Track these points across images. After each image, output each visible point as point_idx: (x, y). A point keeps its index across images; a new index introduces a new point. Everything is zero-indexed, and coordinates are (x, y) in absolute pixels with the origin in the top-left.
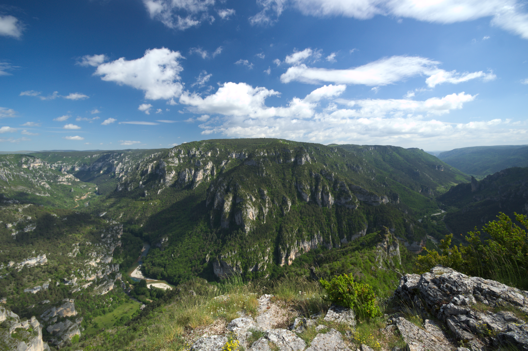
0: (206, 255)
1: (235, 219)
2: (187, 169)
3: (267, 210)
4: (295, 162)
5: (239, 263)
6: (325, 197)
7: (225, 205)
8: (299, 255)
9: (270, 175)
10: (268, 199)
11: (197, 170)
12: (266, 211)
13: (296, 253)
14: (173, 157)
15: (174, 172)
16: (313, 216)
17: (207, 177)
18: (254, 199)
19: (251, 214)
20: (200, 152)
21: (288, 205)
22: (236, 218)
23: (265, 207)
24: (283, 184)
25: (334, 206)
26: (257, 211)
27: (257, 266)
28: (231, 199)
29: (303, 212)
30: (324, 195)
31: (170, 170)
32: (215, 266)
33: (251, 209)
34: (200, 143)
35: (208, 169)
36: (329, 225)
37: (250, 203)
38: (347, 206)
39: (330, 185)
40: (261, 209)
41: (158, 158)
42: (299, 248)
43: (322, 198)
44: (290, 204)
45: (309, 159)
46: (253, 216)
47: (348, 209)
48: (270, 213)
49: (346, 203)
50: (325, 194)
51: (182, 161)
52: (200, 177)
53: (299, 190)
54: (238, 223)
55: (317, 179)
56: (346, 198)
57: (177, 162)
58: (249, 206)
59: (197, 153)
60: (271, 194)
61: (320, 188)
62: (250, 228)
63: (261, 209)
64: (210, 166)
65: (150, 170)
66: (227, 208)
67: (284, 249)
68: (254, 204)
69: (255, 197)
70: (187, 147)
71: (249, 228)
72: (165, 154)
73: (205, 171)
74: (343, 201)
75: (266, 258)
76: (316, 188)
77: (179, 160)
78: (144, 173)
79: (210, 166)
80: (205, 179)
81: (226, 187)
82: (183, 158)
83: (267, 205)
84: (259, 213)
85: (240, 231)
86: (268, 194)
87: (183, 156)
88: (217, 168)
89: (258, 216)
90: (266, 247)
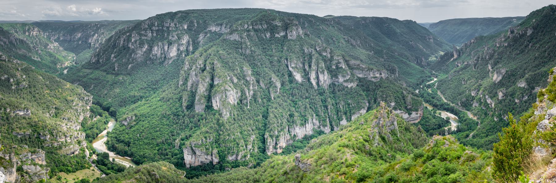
0: (175, 140)
1: (212, 102)
2: (160, 44)
3: (252, 92)
4: (285, 36)
5: (215, 151)
6: (321, 76)
7: (200, 86)
8: (291, 142)
9: (255, 52)
10: (251, 79)
11: (170, 44)
12: (249, 94)
13: (287, 141)
14: (145, 30)
15: (146, 47)
16: (306, 98)
17: (181, 52)
18: (235, 80)
19: (232, 98)
20: (176, 25)
21: (276, 87)
22: (213, 101)
23: (249, 89)
24: (271, 62)
25: (331, 86)
26: (240, 94)
27: (237, 155)
28: (208, 80)
29: (295, 95)
30: (319, 73)
31: (142, 44)
32: (186, 152)
33: (232, 92)
34: (176, 13)
35: (182, 44)
36: (326, 107)
37: (231, 85)
38: (345, 84)
39: (325, 61)
40: (243, 92)
41: (130, 31)
42: (290, 135)
43: (318, 78)
44: (279, 85)
45: (301, 32)
46: (235, 100)
47: (347, 87)
48: (254, 96)
49: (346, 81)
50: (321, 72)
51: (155, 35)
52: (173, 53)
53: (290, 69)
54: (215, 108)
55: (311, 56)
56: (344, 76)
57: (150, 34)
58: (229, 89)
59: (172, 25)
60: (256, 74)
61: (314, 67)
62: (230, 113)
63: (243, 92)
64: (184, 41)
65: (122, 42)
66: (202, 89)
67: (271, 136)
68: (235, 85)
69: (238, 78)
70: (160, 18)
71: (228, 114)
72: (137, 26)
73: (179, 45)
74: (341, 80)
75: (250, 147)
76: (310, 66)
77: (152, 33)
78: (114, 46)
79: (185, 39)
80: (179, 55)
81: (202, 66)
82: (157, 31)
83: (251, 88)
84: (242, 96)
85: (217, 116)
86: (253, 75)
87: (157, 28)
88: (194, 42)
89: (241, 101)
90: (250, 135)
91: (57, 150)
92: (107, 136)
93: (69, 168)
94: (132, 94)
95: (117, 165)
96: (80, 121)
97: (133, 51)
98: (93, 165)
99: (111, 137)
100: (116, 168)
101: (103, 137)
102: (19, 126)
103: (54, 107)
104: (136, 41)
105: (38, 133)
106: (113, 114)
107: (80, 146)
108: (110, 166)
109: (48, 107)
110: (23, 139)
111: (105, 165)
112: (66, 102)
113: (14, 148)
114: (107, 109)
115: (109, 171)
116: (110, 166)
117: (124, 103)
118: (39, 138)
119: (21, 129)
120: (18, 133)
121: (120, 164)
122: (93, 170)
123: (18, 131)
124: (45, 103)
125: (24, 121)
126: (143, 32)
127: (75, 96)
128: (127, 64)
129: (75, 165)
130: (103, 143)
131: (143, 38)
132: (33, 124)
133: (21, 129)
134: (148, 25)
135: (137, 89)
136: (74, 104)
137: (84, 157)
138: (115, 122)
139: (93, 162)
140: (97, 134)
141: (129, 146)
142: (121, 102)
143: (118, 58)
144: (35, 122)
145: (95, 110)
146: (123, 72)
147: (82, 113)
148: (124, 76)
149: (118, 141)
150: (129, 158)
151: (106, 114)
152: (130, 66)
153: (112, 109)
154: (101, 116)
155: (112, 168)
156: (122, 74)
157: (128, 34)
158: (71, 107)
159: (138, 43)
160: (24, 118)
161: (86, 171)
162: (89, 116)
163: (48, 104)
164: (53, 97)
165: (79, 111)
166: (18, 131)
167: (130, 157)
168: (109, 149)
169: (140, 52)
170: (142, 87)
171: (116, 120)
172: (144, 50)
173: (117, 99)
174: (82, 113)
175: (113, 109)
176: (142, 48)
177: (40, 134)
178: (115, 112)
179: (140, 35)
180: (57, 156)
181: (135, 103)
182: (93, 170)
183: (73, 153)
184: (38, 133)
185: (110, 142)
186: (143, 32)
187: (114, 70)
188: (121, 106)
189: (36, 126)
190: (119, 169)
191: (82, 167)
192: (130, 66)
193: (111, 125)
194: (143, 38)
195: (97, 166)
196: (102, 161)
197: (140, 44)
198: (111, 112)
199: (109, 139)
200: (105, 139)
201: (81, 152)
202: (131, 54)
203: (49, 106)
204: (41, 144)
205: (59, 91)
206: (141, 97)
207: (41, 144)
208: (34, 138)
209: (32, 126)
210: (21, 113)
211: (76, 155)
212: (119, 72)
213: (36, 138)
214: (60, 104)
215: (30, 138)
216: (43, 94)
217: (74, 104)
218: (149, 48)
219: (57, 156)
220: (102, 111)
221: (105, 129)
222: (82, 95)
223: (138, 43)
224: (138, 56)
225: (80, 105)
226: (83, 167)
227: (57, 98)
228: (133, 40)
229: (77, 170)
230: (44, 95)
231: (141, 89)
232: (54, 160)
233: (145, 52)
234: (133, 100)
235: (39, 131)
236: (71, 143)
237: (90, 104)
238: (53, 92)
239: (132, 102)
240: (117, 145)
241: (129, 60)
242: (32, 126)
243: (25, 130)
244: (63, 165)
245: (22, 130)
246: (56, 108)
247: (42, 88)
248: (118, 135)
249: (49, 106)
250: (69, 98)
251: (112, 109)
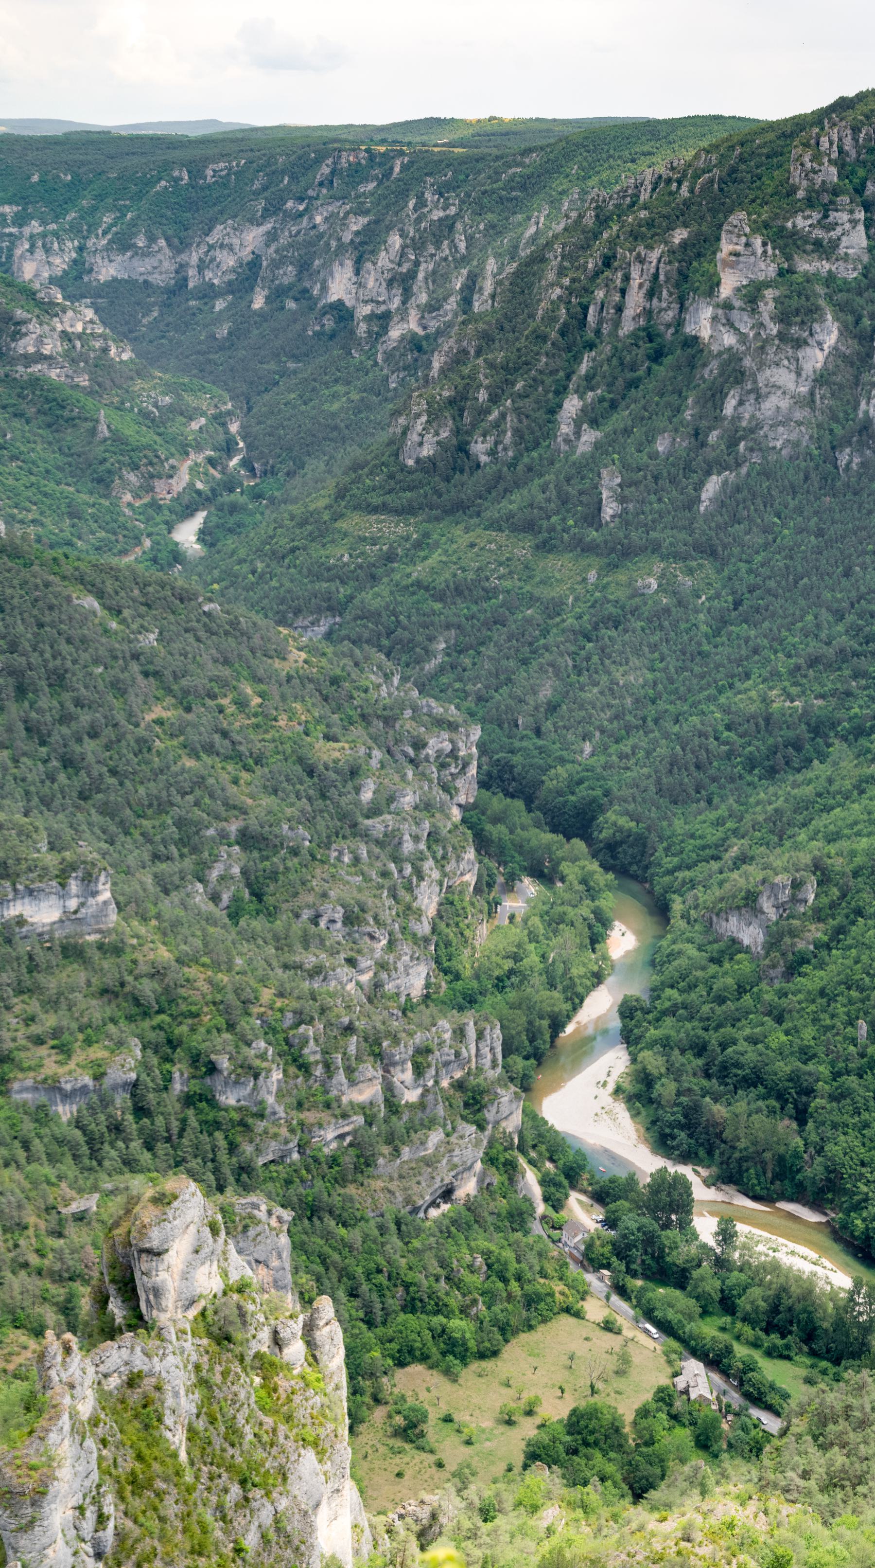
91: (341, 1180)
92: (630, 1038)
93: (458, 1325)
94: (747, 699)
95: (756, 1274)
96: (424, 928)
97: (734, 372)
98: (590, 1278)
99: (666, 1044)
100: (755, 1298)
101: (585, 1049)
102: (50, 1021)
103: (233, 828)
104: (752, 295)
105: (195, 1059)
106: (627, 861)
107: (481, 1127)
108: (708, 1281)
109: (189, 838)
110: (99, 1125)
111: (678, 1277)
112: (308, 786)
113: (80, 1218)
114: (576, 822)
115: (709, 1330)
116: (708, 1281)
117: (691, 779)
118: (212, 1102)
119: (64, 1050)
120: (53, 1087)
121: (775, 1267)
122: (608, 1327)
123: (51, 1067)
124: (162, 806)
125: (74, 975)
126: (801, 222)
127: (358, 731)
128: (691, 468)
129: (491, 1297)
130: (605, 1096)
131: (805, 266)
132: (148, 988)
133: (64, 1050)
134: (841, 164)
135: (782, 663)
136: (367, 796)
137: (518, 1218)
138: (650, 925)
139: (591, 1260)
140: (557, 1025)
141: (801, 1117)
142: (673, 763)
143: (619, 419)
144: (157, 973)
145: (498, 831)
146: (666, 537)
147: (428, 864)
148: (676, 568)
149: (723, 1072)
150: (813, 1217)
151: (578, 861)
152: (712, 486)
153: (614, 820)
154: (544, 874)
155: (727, 1304)
156: (655, 548)
157: (679, 235)
158: (349, 825)
159: (767, 307)
160: (72, 952)
161: (560, 1334)
162: (470, 878)
163: (184, 806)
164: (210, 749)
165: (408, 846)
166: (51, 1067)
167: (816, 1205)
168: (662, 1141)
169: (783, 377)
170: (814, 647)
171: (661, 910)
172: (815, 359)
173: (638, 739)
174: (428, 864)
175: (624, 822)
176: (799, 344)
177: (212, 1069)
178: (641, 842)
179: (787, 242)
180: (354, 1236)
181: (772, 773)
182: (608, 1327)
183: (447, 1194)
184: (195, 1059)
185: (666, 1089)
186: (801, 222)
187: (593, 517)
188: (677, 798)
189: (168, 1000)
190: (775, 1309)
191: (531, 1301)
192: (712, 486)
193: (622, 942)
194: (805, 266)
195: (621, 1291)
196: (650, 1240)
197: (783, 317)
198: (612, 847)
199: (652, 1060)
200: (614, 1062)
201: (496, 1178)
202: (715, 397)
203: (200, 826)
204: (233, 1148)
205: (241, 704)
206: (820, 729)
207: (233, 1148)
208: (171, 1101)
209: (140, 1009)
210: (43, 913)
211: (470, 1206)
212: (636, 536)
213: (188, 1100)
214: (268, 801)
215: (141, 1111)
216: (132, 733)
217: (367, 796)
218: (851, 347)
219: (354, 1236)
220: (548, 837)
221: (598, 978)
222: (407, 723)
223: (767, 307)
224: (773, 403)
225: (408, 800)
226: (536, 1309)
227: (236, 757)
228: (729, 284)
229: (506, 1331)
230: (143, 746)
231: (814, 662)
232: (344, 1273)
233: (821, 379)
234: (756, 747)
235: (197, 1041)
236: (422, 1118)
237: (467, 790)
238: (202, 716)
239: (751, 764)
240: (719, 1110)
241: (698, 435)
242: (140, 1009)
243: (97, 1052)
244: (410, 1306)
245: (79, 1056)
246: (246, 839)
247: (119, 688)
248: (708, 1024)
249: (200, 826)
250: (327, 753)
251: (614, 820)
